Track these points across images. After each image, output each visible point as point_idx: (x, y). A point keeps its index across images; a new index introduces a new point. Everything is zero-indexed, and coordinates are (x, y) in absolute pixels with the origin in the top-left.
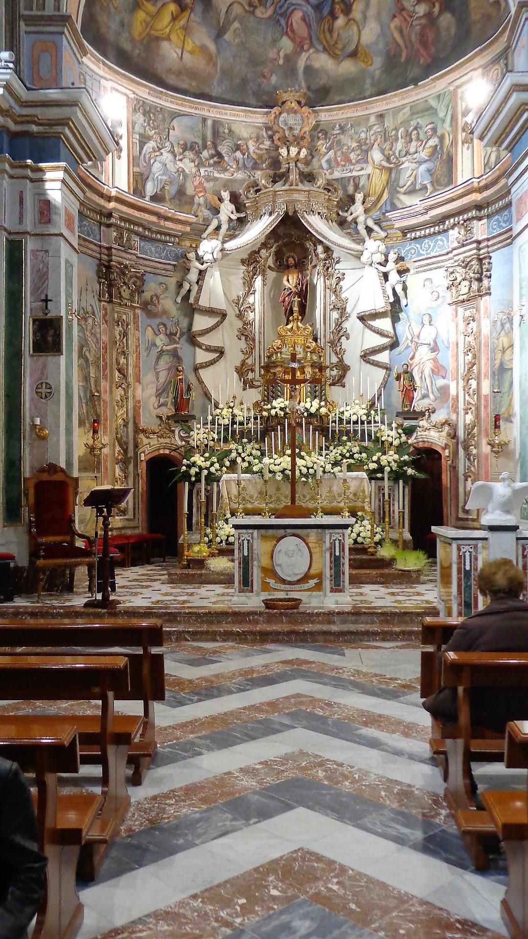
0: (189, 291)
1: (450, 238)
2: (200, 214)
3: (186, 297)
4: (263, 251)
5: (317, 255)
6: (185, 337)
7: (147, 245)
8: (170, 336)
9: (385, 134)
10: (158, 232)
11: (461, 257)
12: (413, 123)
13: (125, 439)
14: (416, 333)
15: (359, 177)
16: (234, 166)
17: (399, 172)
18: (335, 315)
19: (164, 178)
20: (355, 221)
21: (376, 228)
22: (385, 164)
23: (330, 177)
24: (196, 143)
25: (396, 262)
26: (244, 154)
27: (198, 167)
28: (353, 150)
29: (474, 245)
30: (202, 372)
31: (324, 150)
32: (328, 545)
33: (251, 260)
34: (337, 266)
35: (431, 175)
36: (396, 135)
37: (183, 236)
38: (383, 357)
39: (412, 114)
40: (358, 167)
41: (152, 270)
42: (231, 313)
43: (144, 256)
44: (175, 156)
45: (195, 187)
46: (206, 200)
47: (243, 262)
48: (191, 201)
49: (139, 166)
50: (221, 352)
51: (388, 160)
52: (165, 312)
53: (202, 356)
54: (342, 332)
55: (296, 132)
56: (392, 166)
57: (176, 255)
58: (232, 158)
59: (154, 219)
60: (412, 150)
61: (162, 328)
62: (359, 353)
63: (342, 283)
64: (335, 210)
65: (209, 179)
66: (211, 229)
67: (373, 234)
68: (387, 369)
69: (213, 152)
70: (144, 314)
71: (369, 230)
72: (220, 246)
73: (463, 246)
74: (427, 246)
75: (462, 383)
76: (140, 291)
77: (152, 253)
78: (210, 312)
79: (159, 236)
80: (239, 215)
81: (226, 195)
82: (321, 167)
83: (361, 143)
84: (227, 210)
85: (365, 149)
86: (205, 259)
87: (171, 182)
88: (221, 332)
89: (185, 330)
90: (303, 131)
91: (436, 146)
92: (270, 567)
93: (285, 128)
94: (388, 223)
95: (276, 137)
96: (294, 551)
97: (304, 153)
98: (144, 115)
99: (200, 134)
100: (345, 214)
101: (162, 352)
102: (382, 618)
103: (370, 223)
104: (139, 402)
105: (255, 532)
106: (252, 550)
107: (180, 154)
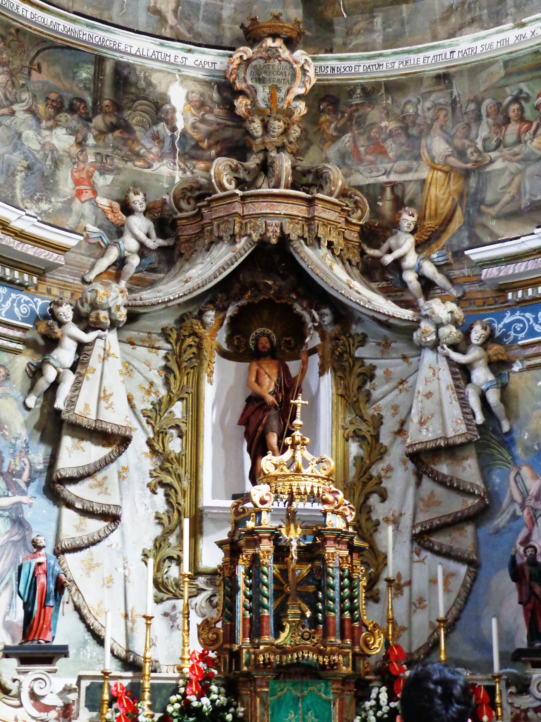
0: (55, 385)
12: (511, 91)
15: (403, 184)
20: (398, 265)
22: (454, 161)
24: (82, 101)
25: (484, 345)
28: (391, 135)
31: (331, 130)
39: (508, 75)
51: (461, 154)
56: (469, 165)
68: (470, 563)
89: (40, 467)
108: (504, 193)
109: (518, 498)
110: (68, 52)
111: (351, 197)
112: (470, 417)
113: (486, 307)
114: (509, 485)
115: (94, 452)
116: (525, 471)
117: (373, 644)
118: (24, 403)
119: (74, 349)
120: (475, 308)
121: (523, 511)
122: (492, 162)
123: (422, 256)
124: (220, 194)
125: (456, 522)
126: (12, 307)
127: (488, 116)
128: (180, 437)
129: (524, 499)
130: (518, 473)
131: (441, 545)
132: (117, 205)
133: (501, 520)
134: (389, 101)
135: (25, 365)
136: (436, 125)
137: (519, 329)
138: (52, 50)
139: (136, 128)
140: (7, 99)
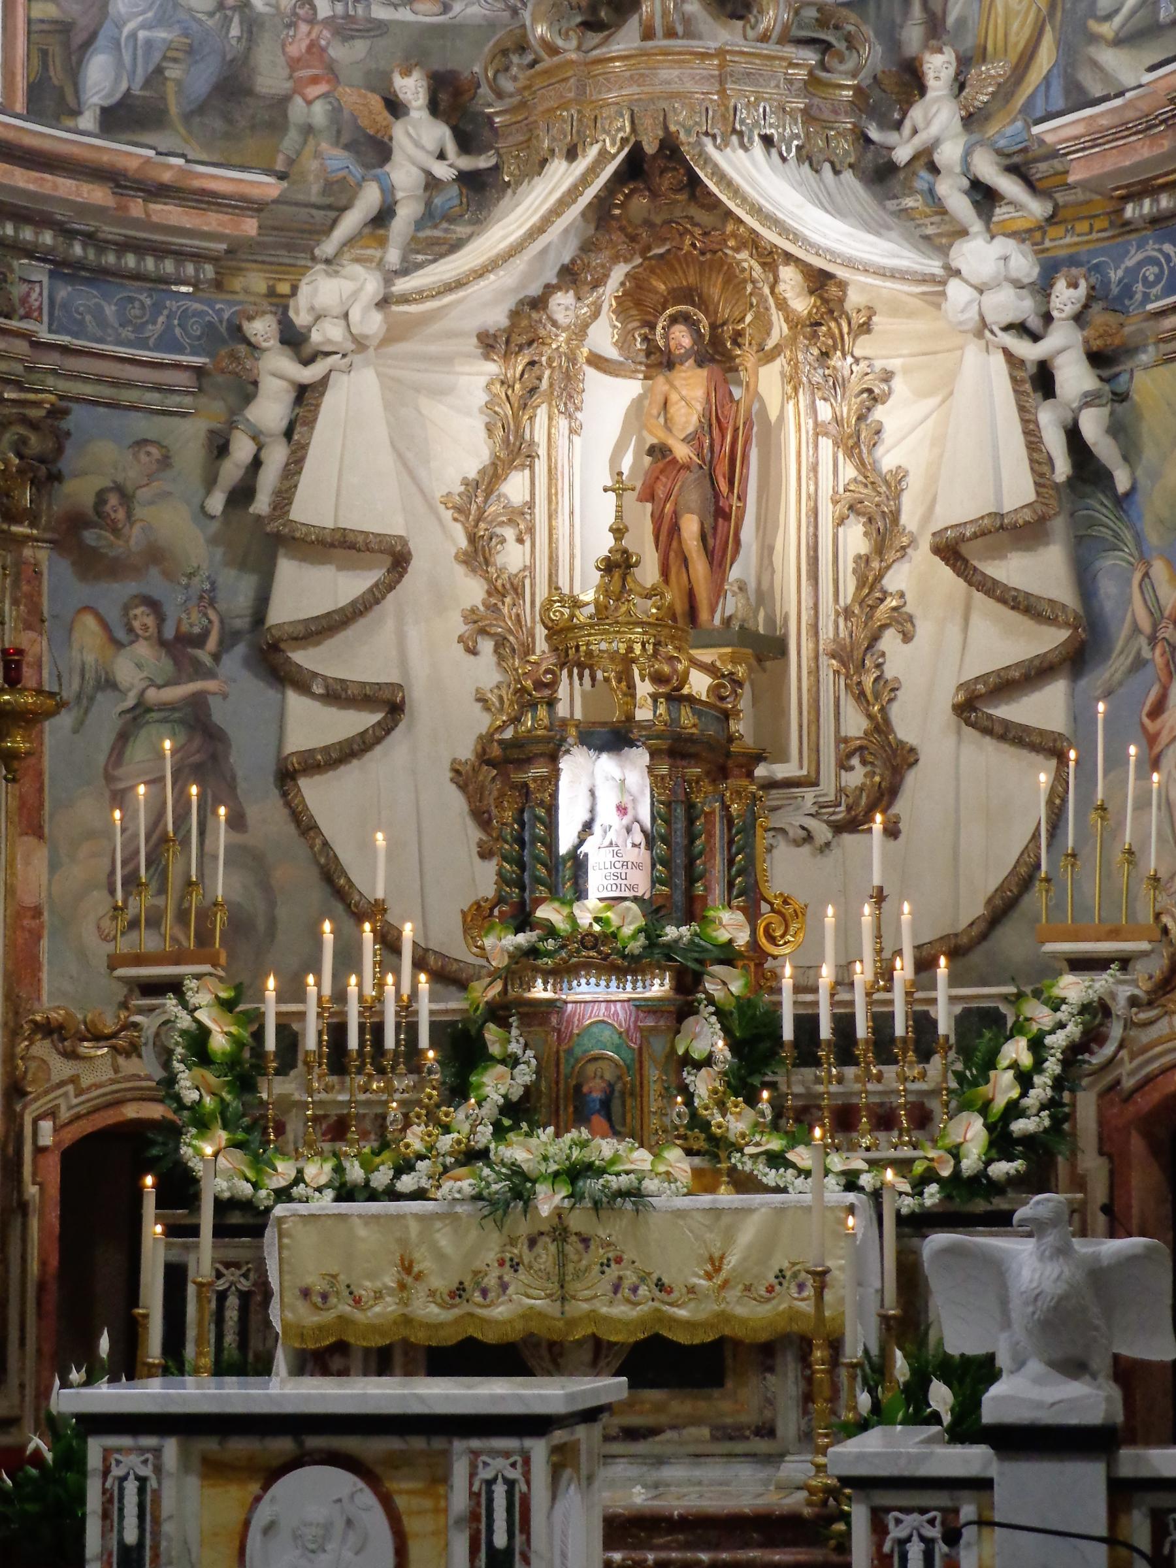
3: (242, 494)
4: (563, 304)
5: (782, 305)
6: (240, 649)
7: (81, 298)
8: (180, 648)
10: (125, 246)
18: (856, 539)
19: (162, 34)
20: (927, 160)
21: (1009, 186)
25: (1079, 318)
32: (459, 1501)
33: (518, 332)
37: (233, 257)
38: (1044, 709)
41: (106, 392)
42: (438, 545)
43: (64, 339)
45: (294, 64)
47: (488, 343)
50: (391, 705)
52: (155, 555)
53: (310, 724)
59: (97, 195)
61: (142, 618)
62: (946, 696)
63: (879, 413)
66: (351, 221)
67: (1001, 213)
70: (64, 566)
71: (984, 196)
72: (372, 285)
76: (45, 473)
77: (102, 322)
78: (339, 546)
79: (131, 261)
80: (467, 163)
81: (412, 88)
84: (421, 144)
86: (316, 337)
87: (190, 51)
88: (390, 625)
89: (242, 623)
94: (1057, 164)
96: (327, 1527)
100: (891, 138)
103: (988, 170)
104: (37, 912)
105: (171, 1447)
106: (156, 1521)
109: (1145, 624)
112: (1045, 469)
113: (1095, 236)
114: (1130, 601)
115: (343, 586)
116: (1159, 569)
117: (783, 936)
118: (202, 507)
119: (290, 397)
120: (1076, 239)
121: (1153, 649)
123: (976, 137)
124: (548, 62)
125: (1034, 675)
126: (169, 327)
128: (520, 541)
129: (1155, 626)
130: (1146, 575)
131: (1007, 724)
132: (376, 102)
133: (1115, 666)
135: (202, 434)
137: (1151, 278)
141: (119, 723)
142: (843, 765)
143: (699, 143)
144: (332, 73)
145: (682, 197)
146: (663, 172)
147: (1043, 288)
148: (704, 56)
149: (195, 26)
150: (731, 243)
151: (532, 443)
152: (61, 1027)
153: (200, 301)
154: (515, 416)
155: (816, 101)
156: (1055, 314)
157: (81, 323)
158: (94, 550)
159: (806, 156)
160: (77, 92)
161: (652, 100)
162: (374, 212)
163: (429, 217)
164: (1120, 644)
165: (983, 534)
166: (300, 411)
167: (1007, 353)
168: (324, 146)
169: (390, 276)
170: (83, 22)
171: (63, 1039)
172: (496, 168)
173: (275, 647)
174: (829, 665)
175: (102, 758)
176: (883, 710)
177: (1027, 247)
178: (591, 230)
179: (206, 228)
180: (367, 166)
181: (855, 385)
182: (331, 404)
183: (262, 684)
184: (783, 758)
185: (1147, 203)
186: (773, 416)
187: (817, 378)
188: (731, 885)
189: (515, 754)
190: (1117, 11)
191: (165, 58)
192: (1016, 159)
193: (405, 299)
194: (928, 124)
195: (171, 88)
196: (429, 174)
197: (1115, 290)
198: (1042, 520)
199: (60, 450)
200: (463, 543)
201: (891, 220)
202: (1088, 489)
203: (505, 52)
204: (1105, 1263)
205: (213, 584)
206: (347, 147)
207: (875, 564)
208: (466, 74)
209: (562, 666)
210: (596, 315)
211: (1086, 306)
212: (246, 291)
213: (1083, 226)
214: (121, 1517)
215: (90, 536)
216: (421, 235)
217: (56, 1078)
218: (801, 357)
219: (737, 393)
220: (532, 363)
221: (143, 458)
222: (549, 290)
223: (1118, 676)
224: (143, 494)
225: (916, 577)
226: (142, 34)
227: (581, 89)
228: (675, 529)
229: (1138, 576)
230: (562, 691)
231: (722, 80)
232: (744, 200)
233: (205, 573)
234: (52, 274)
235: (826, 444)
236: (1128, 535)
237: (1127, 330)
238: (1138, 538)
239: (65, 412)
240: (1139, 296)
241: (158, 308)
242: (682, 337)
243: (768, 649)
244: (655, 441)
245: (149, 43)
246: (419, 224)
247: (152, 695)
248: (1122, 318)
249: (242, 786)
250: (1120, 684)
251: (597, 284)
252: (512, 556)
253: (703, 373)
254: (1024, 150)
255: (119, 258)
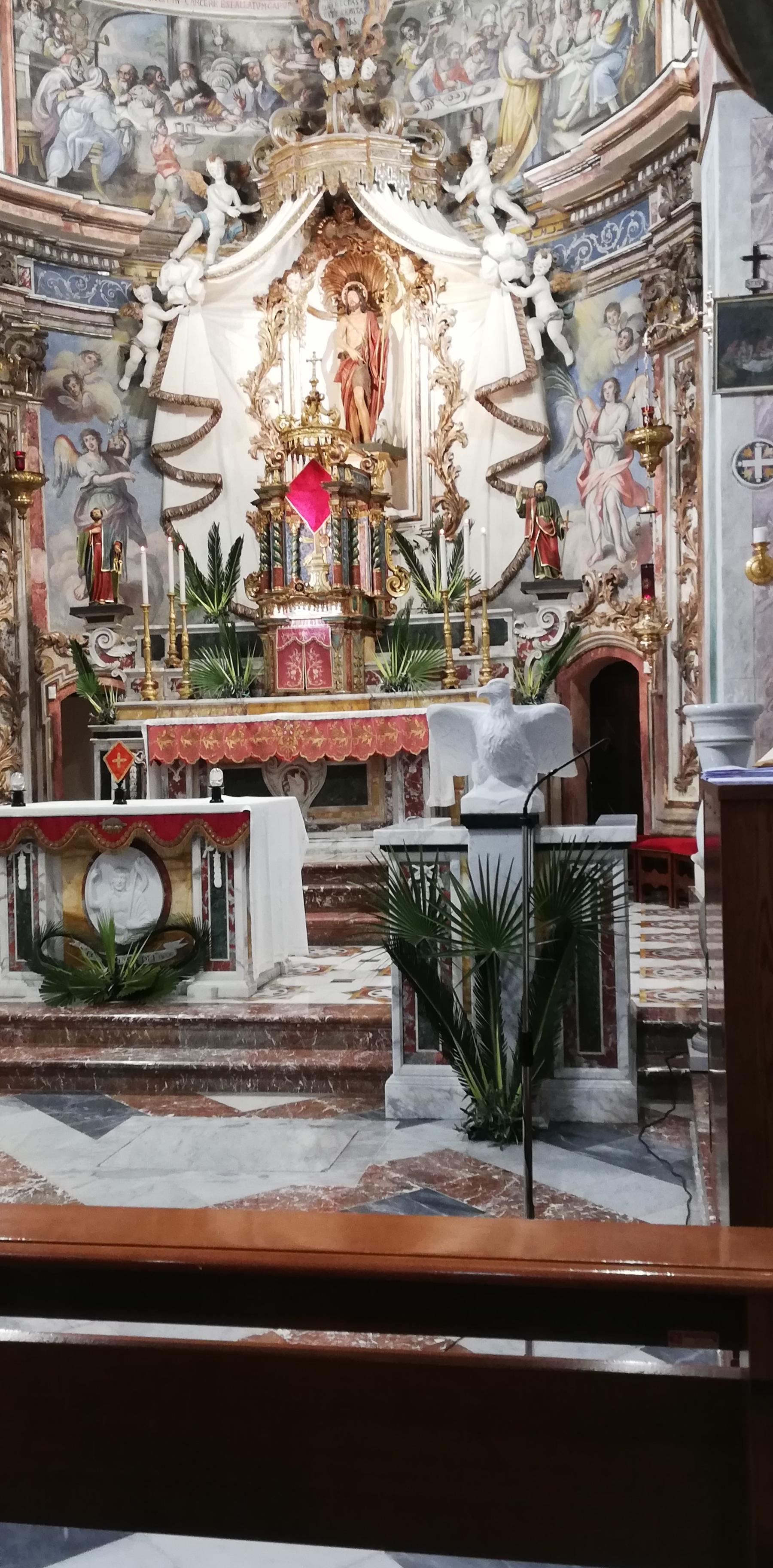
1: (652, 211)
2: (167, 211)
3: (137, 378)
4: (294, 279)
5: (402, 278)
6: (140, 457)
8: (110, 456)
9: (530, 10)
10: (72, 250)
11: (664, 248)
13: (12, 659)
14: (591, 423)
15: (481, 108)
16: (237, 111)
17: (556, 86)
18: (439, 397)
19: (88, 141)
20: (472, 199)
21: (513, 210)
23: (423, 115)
24: (157, 69)
25: (548, 276)
26: (255, 85)
27: (161, 115)
28: (470, 54)
29: (690, 217)
30: (177, 525)
31: (413, 60)
33: (274, 297)
34: (442, 298)
35: (616, 82)
36: (551, 10)
37: (128, 257)
40: (479, 87)
44: (112, 97)
45: (157, 158)
46: (180, 182)
47: (258, 302)
48: (148, 186)
49: (30, 119)
51: (536, 64)
52: (96, 409)
54: (452, 433)
55: (355, 28)
56: (544, 75)
57: (119, 294)
58: (231, 94)
59: (55, 220)
60: (581, 35)
61: (90, 441)
63: (450, 332)
64: (433, 181)
65: (183, 139)
66: (189, 239)
67: (510, 225)
69: (193, 85)
70: (49, 414)
71: (502, 216)
73: (671, 220)
74: (609, 235)
75: (672, 517)
78: (185, 404)
79: (76, 257)
81: (216, 169)
82: (409, 97)
83: (484, 37)
84: (223, 198)
85: (491, 46)
86: (170, 297)
87: (103, 150)
89: (140, 444)
90: (369, 25)
91: (625, 18)
92: (80, 913)
93: (332, 21)
95: (315, 44)
97: (369, 68)
98: (42, 12)
99: (164, 50)
101: (91, 489)
102: (284, 1033)
104: (43, 586)
106: (36, 877)
107: (123, 93)
108: (575, 101)
109: (580, 433)
110: (136, 17)
111: (428, 131)
112: (530, 353)
113: (556, 233)
114: (571, 421)
116: (587, 404)
119: (160, 328)
122: (563, 67)
123: (497, 185)
125: (525, 460)
127: (561, 12)
128: (277, 402)
130: (580, 406)
132: (199, 177)
133: (564, 456)
134: (469, 14)
135: (117, 349)
136: (513, 33)
138: (119, 19)
139: (215, 89)
140: (73, 79)
141: (80, 493)
142: (434, 510)
143: (357, 189)
144: (177, 163)
145: (352, 223)
146: (344, 209)
147: (529, 261)
148: (359, 141)
149: (105, 137)
150: (377, 247)
151: (280, 353)
152: (57, 641)
153: (114, 280)
154: (273, 339)
155: (417, 169)
156: (536, 273)
157: (53, 290)
158: (64, 406)
159: (411, 197)
160: (45, 170)
161: (333, 166)
162: (200, 235)
163: (227, 237)
164: (567, 443)
165: (500, 388)
166: (165, 335)
167: (512, 295)
168: (174, 200)
169: (207, 267)
170: (47, 133)
171: (59, 648)
172: (260, 212)
173: (157, 455)
174: (427, 460)
175: (73, 511)
176: (452, 481)
177: (521, 238)
178: (308, 243)
179: (112, 240)
180: (196, 211)
181: (438, 318)
182: (179, 332)
183: (151, 475)
184: (404, 507)
185: (582, 211)
186: (399, 339)
187: (420, 315)
188: (373, 562)
189: (264, 496)
190: (567, 113)
191: (90, 153)
192: (518, 196)
193: (214, 277)
194: (473, 178)
195: (94, 170)
196: (226, 213)
197: (566, 261)
198: (529, 380)
199: (44, 354)
200: (249, 404)
201: (456, 232)
202: (552, 365)
203: (262, 149)
204: (532, 719)
205: (125, 424)
206: (185, 201)
207: (449, 409)
208: (244, 163)
209: (288, 452)
210: (311, 287)
211: (551, 269)
212: (136, 275)
213: (550, 229)
214: (17, 875)
215: (61, 399)
216: (224, 246)
217: (56, 667)
218: (411, 304)
219: (381, 326)
220: (280, 312)
221: (88, 360)
222: (287, 273)
223: (566, 459)
224: (88, 378)
225: (470, 415)
226: (78, 140)
227: (298, 161)
228: (351, 394)
229: (576, 408)
230: (288, 464)
231: (368, 155)
232: (380, 218)
233: (121, 419)
234: (35, 264)
235: (424, 348)
236: (571, 387)
237: (572, 281)
238: (576, 389)
239: (47, 335)
240: (578, 263)
241: (91, 284)
242: (353, 298)
243: (398, 455)
244: (342, 351)
245: (82, 146)
246: (223, 241)
247: (97, 480)
248: (569, 275)
249: (144, 525)
250: (567, 463)
251: (311, 271)
252: (273, 411)
253: (365, 315)
254: (521, 191)
255: (70, 256)
